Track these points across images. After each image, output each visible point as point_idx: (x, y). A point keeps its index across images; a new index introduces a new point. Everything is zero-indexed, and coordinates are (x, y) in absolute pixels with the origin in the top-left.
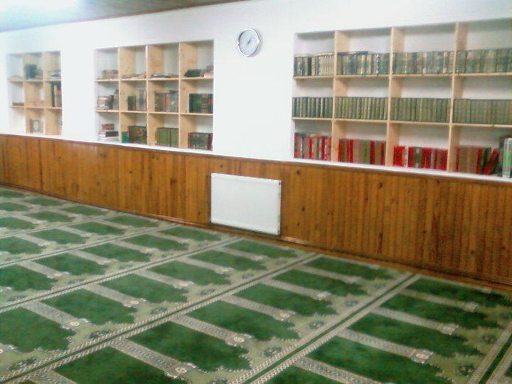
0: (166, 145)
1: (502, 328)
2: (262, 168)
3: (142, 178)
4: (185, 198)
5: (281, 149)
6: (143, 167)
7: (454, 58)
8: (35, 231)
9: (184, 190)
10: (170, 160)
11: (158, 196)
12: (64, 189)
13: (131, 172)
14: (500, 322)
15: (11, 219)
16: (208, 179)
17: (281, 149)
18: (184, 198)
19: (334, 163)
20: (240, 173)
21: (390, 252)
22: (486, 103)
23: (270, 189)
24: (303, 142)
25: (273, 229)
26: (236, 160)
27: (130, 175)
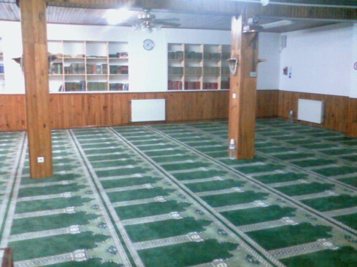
0: (79, 91)
1: (13, 165)
2: (155, 95)
3: (83, 109)
4: (113, 114)
5: (164, 88)
6: (83, 103)
7: (221, 55)
8: (129, 150)
9: (112, 110)
10: (103, 97)
11: (94, 117)
12: (7, 125)
13: (74, 106)
14: (11, 163)
15: (117, 149)
16: (130, 103)
17: (164, 88)
18: (112, 115)
19: (183, 90)
20: (145, 98)
21: (205, 117)
22: (7, 97)
23: (161, 103)
24: (171, 84)
25: (163, 118)
26: (141, 93)
27: (73, 108)
